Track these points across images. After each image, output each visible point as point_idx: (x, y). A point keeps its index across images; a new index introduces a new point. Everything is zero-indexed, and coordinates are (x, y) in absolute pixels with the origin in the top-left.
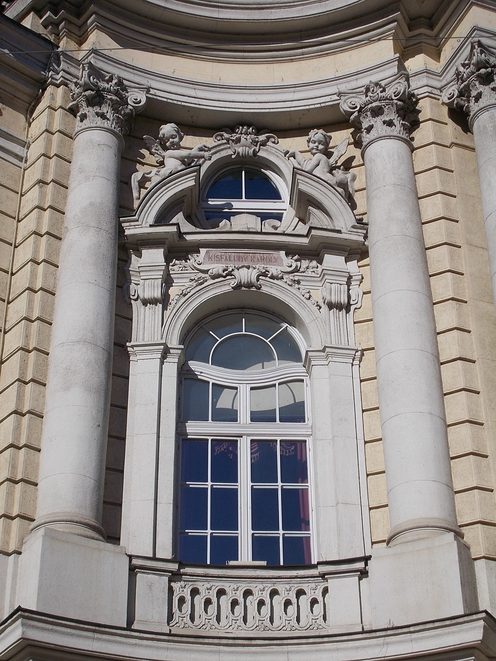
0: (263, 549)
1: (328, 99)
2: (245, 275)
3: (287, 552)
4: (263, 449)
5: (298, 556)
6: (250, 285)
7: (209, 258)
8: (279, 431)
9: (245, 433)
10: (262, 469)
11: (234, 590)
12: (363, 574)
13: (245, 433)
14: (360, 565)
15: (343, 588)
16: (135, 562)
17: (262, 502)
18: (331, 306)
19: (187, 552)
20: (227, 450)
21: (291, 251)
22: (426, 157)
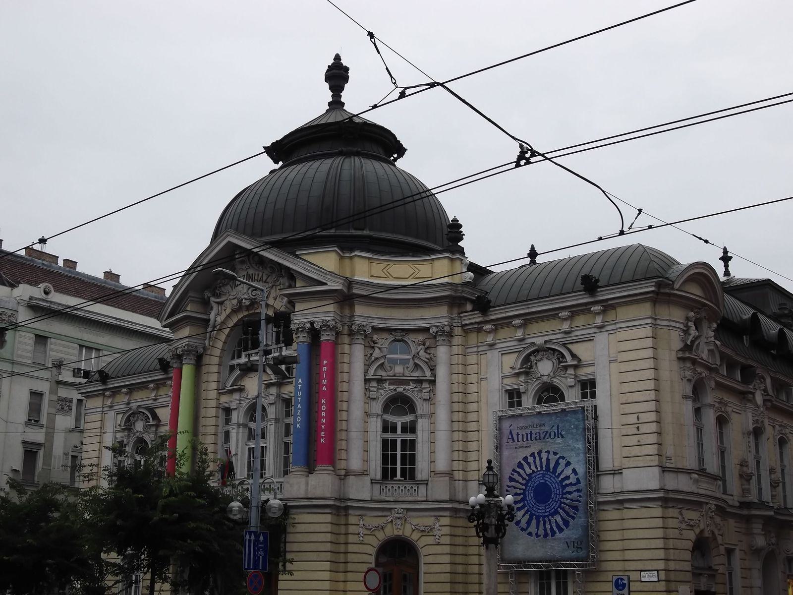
0: (403, 471)
1: (427, 325)
2: (400, 390)
3: (409, 474)
4: (404, 442)
5: (412, 476)
6: (401, 393)
7: (390, 384)
8: (409, 436)
9: (399, 436)
10: (403, 448)
11: (396, 487)
12: (427, 484)
13: (399, 436)
14: (427, 482)
15: (422, 489)
16: (372, 481)
17: (403, 457)
18: (424, 399)
19: (384, 471)
20: (394, 442)
21: (414, 381)
22: (456, 350)
